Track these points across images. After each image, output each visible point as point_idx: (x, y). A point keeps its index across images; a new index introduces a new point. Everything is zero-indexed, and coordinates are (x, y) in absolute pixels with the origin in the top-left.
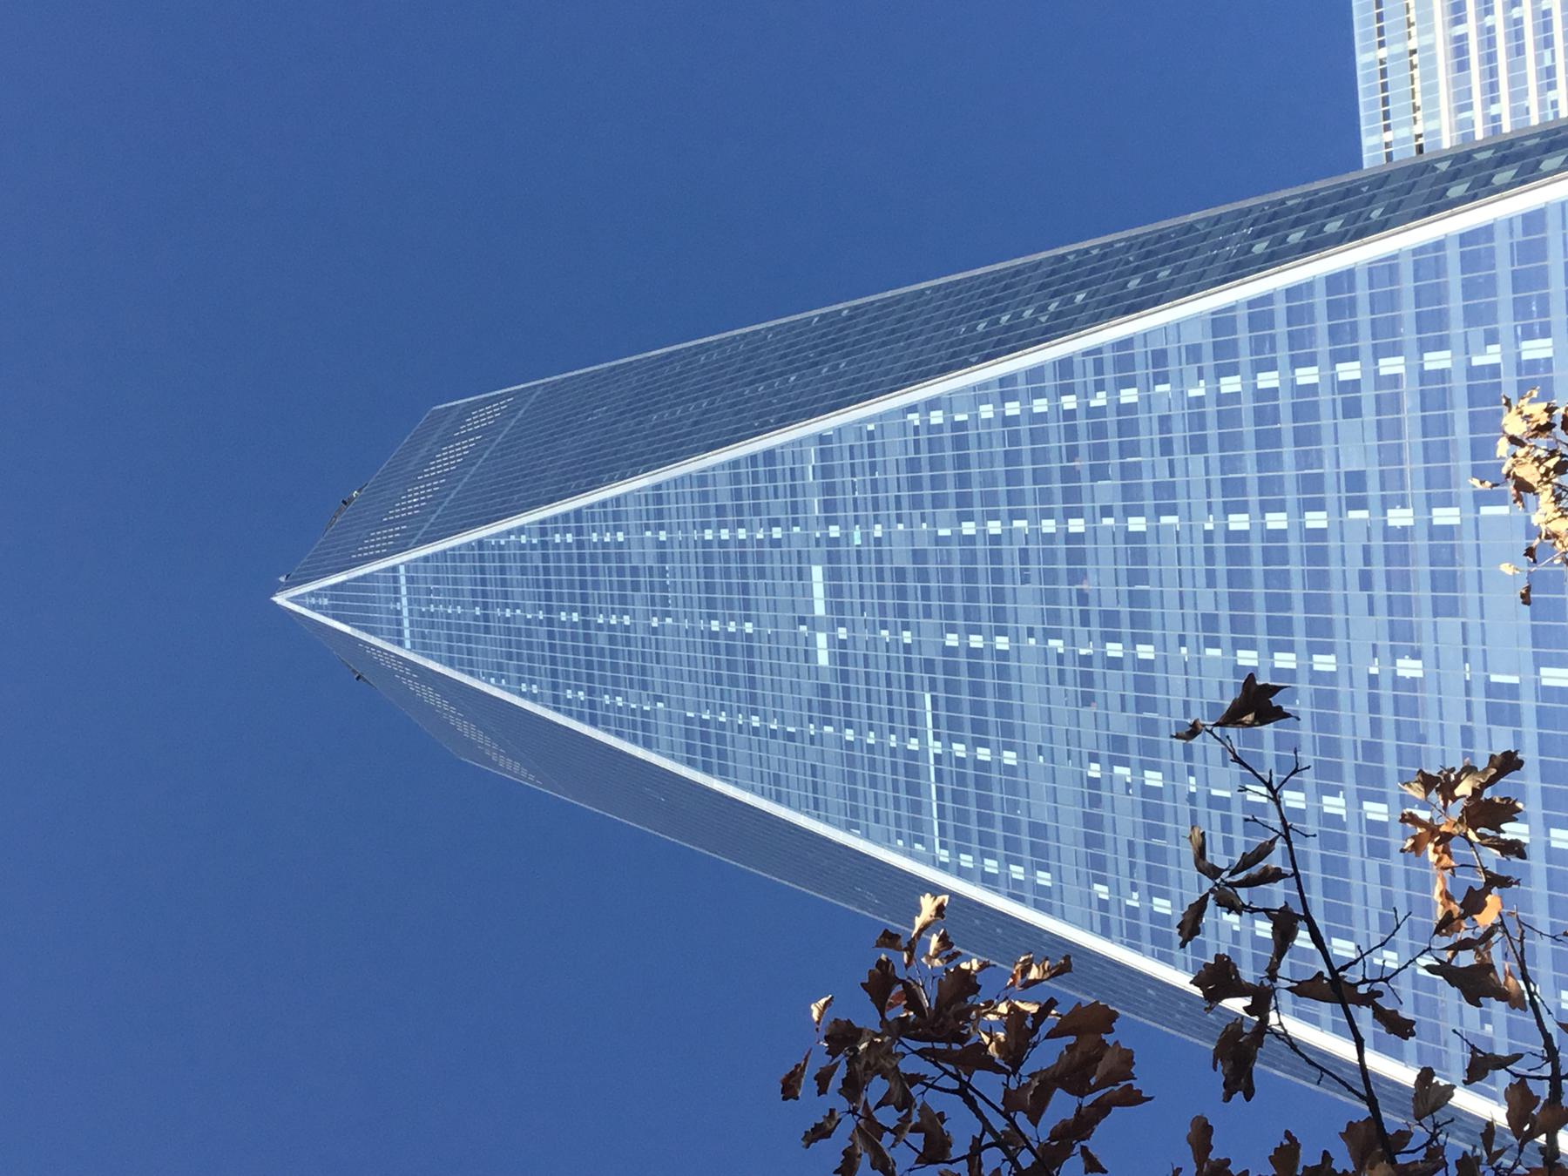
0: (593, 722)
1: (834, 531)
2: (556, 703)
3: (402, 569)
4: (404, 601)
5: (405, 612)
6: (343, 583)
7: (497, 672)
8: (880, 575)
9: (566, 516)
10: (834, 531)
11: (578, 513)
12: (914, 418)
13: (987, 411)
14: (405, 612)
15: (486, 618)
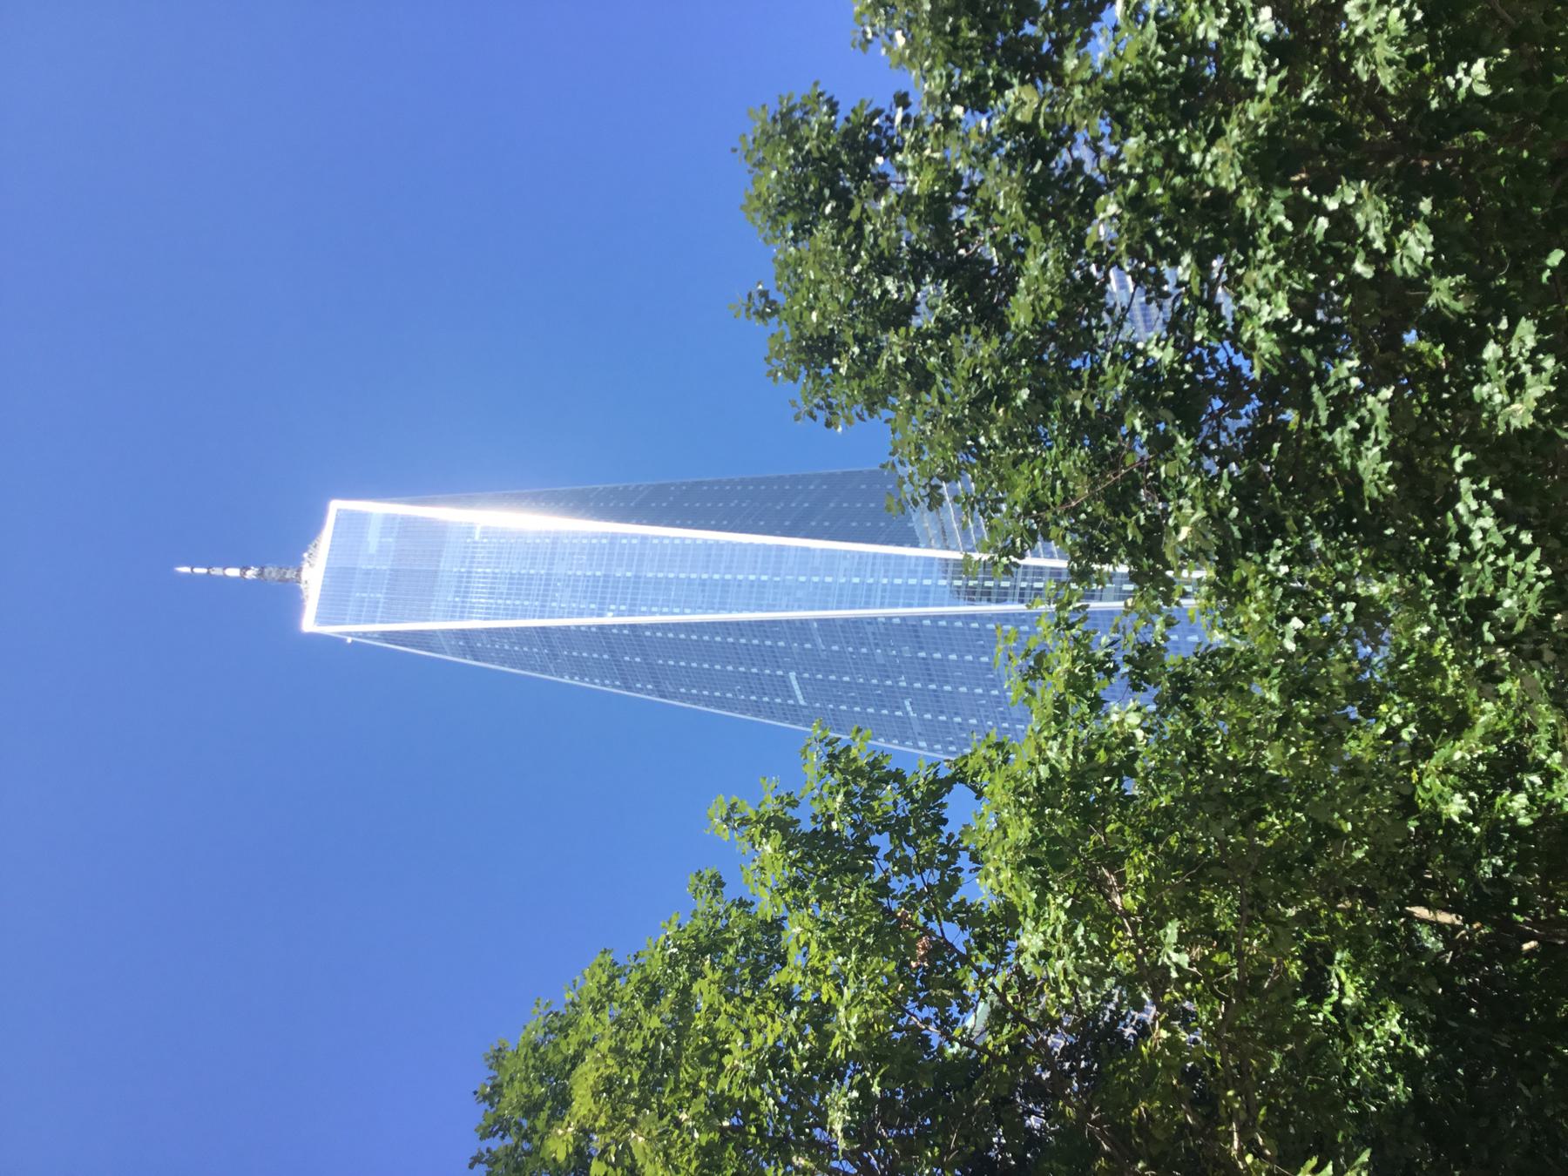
2: (629, 689)
13: (927, 622)
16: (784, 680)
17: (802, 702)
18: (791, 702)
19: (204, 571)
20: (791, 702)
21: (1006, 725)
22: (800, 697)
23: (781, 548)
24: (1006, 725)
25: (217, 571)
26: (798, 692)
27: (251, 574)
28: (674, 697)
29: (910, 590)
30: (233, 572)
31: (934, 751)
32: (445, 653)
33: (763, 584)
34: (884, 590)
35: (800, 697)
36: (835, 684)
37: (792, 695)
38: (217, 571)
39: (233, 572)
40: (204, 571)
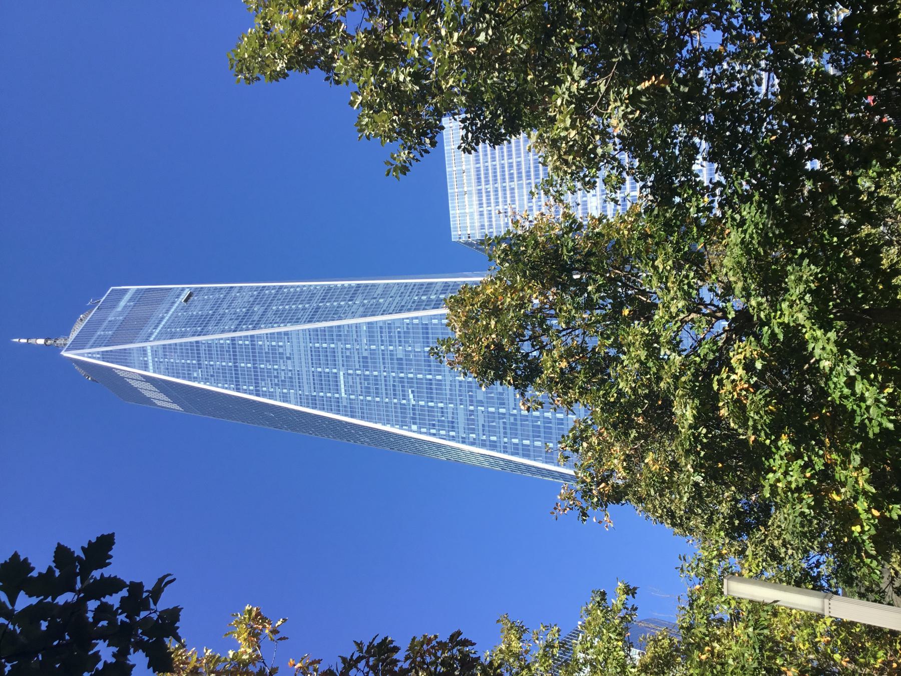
0: (258, 395)
1: (373, 347)
2: (238, 390)
3: (149, 348)
4: (150, 358)
5: (150, 361)
6: (111, 351)
7: (206, 380)
8: (392, 359)
9: (247, 337)
10: (373, 347)
11: (252, 336)
12: (408, 321)
13: (435, 321)
14: (150, 361)
15: (199, 364)
16: (336, 376)
17: (343, 395)
18: (337, 395)
19: (25, 341)
20: (337, 395)
21: (472, 408)
22: (343, 390)
23: (359, 286)
24: (472, 408)
25: (32, 341)
26: (343, 386)
27: (49, 342)
28: (264, 396)
29: (429, 301)
30: (41, 341)
31: (421, 433)
32: (134, 367)
33: (339, 306)
34: (413, 302)
35: (343, 390)
36: (366, 378)
37: (338, 391)
38: (32, 341)
39: (41, 341)
40: (25, 341)
